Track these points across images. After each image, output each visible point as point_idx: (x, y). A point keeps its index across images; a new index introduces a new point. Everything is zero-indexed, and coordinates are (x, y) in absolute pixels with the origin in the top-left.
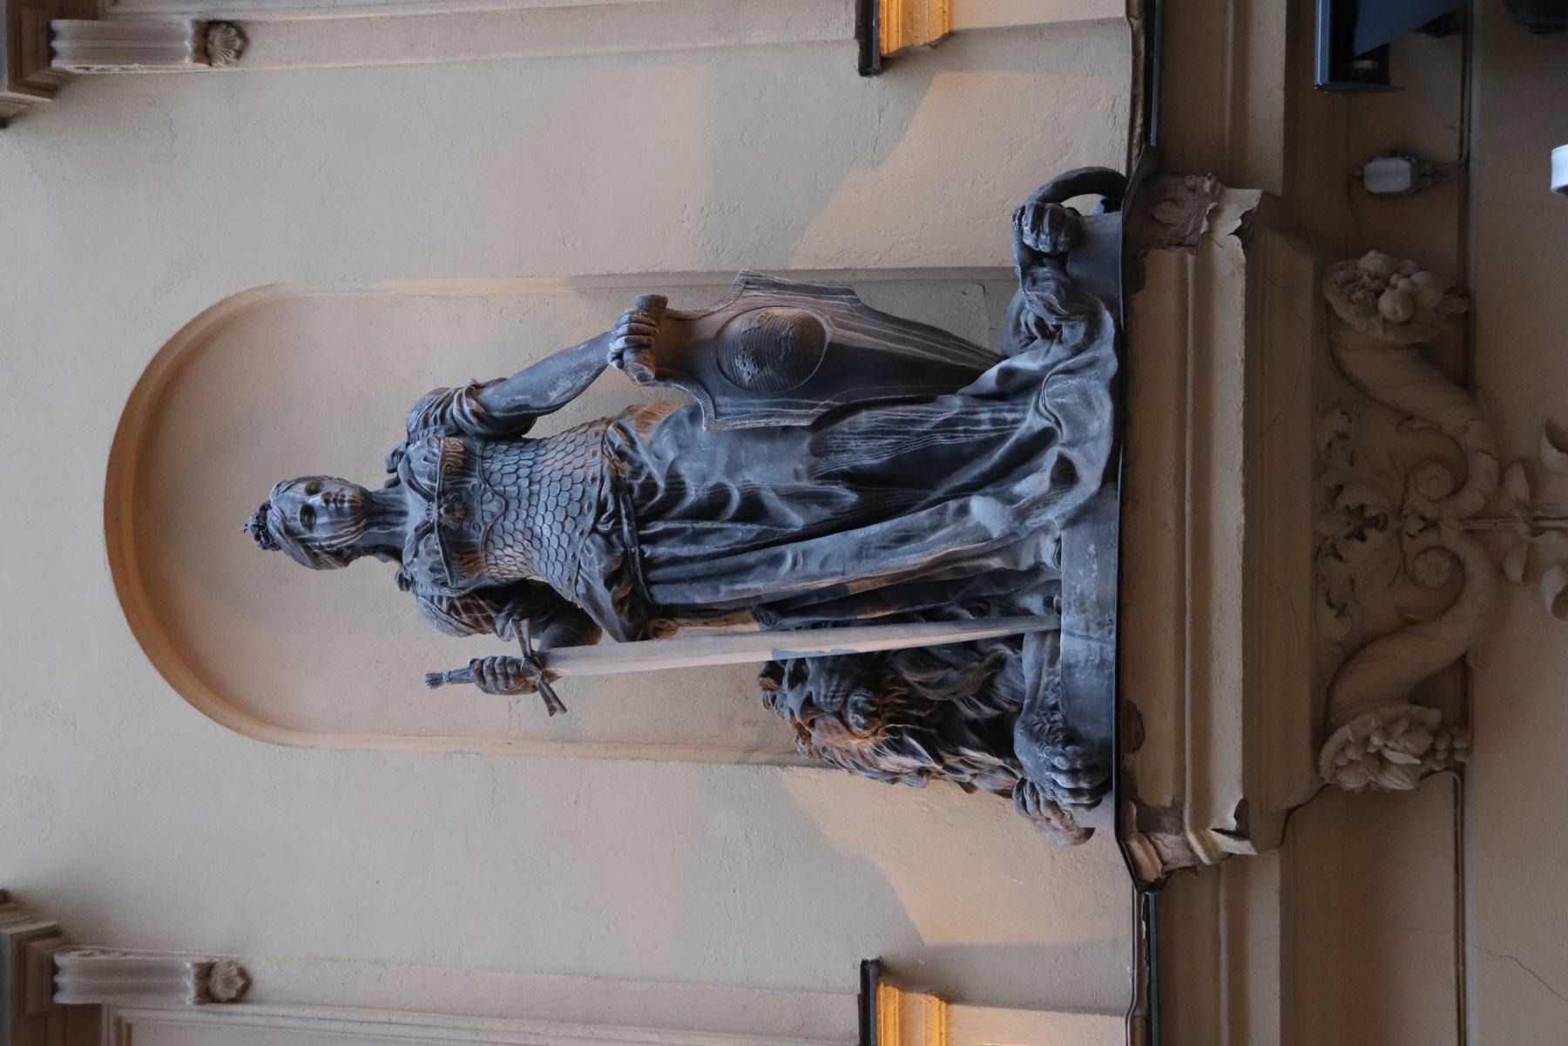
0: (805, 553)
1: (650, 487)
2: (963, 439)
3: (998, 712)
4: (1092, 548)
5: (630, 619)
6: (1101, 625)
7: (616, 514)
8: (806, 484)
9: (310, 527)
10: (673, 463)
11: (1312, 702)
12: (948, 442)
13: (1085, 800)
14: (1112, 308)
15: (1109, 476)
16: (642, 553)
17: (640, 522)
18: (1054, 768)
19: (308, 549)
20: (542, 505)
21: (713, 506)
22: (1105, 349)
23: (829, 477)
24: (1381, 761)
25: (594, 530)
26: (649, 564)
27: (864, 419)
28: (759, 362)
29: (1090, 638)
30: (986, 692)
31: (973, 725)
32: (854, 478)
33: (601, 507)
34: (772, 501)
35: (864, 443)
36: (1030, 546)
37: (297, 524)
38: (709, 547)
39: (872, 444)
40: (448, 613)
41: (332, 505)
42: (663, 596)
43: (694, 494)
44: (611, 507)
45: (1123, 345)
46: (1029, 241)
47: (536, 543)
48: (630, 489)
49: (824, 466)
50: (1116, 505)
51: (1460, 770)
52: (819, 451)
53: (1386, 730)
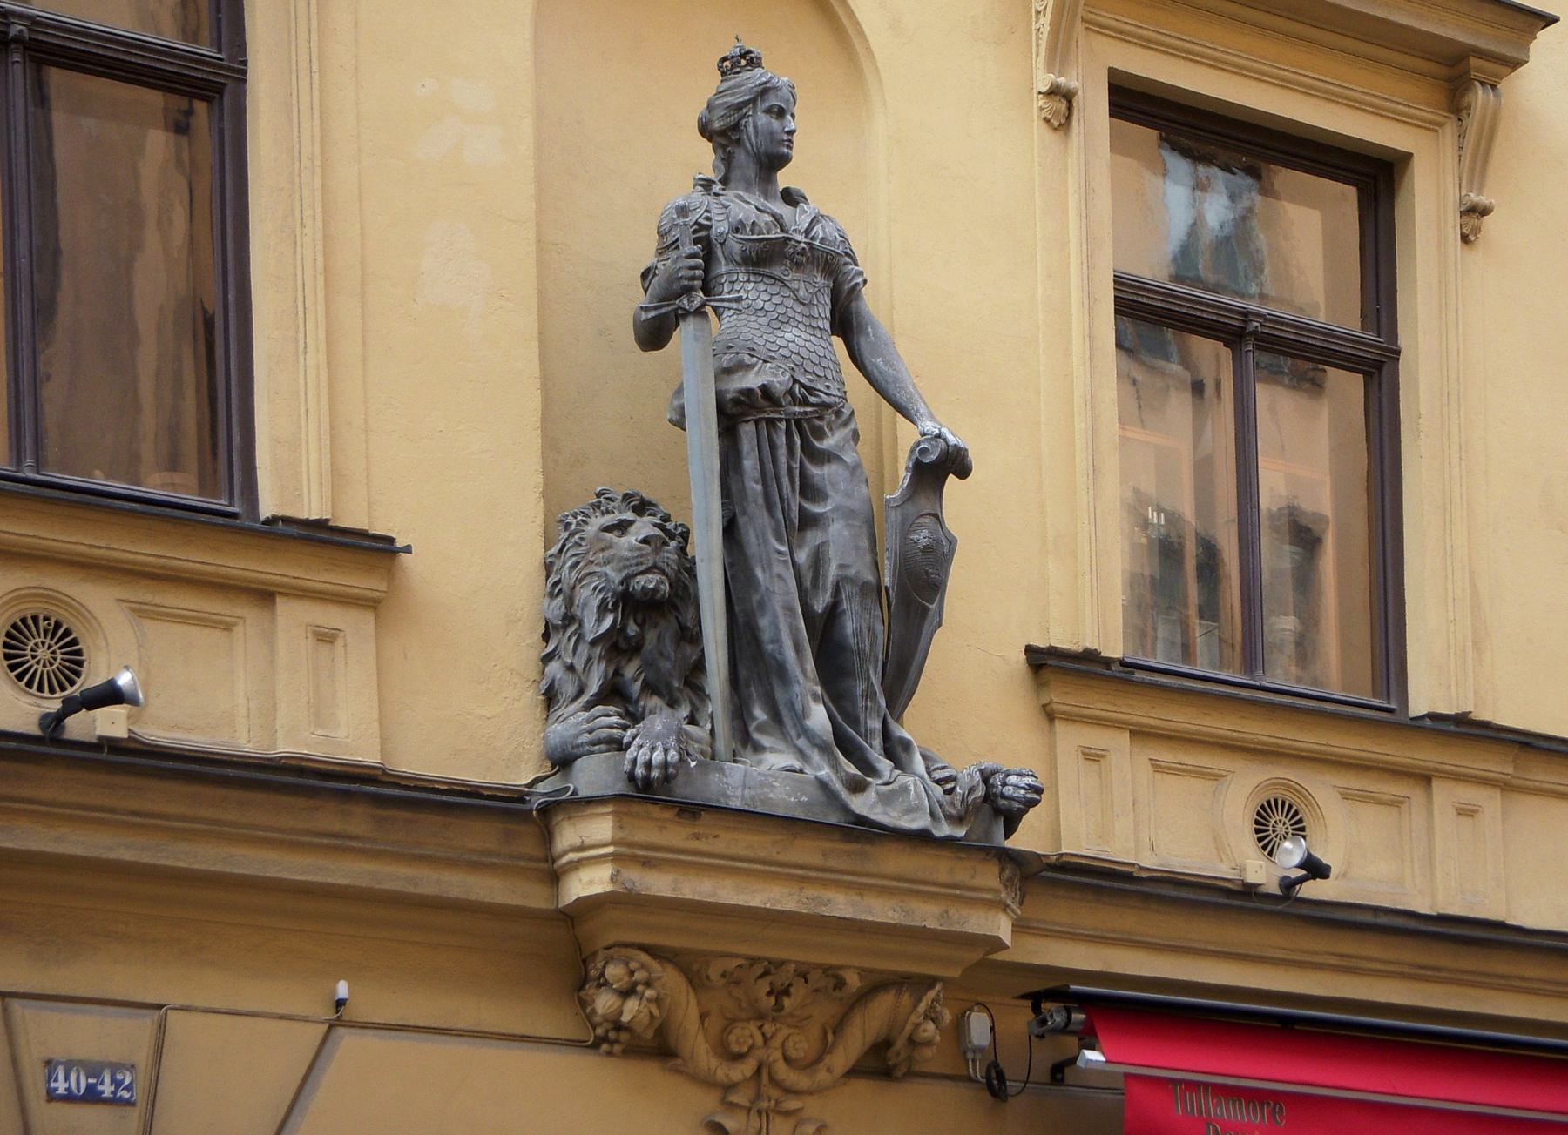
0: (785, 562)
1: (820, 435)
2: (860, 703)
3: (635, 696)
4: (804, 799)
5: (732, 399)
6: (752, 798)
7: (805, 402)
8: (832, 571)
9: (768, 111)
10: (840, 459)
11: (681, 945)
12: (859, 692)
13: (639, 771)
14: (965, 838)
15: (861, 820)
16: (780, 420)
17: (798, 423)
18: (653, 749)
19: (746, 103)
20: (808, 337)
21: (809, 490)
22: (944, 830)
23: (837, 591)
24: (627, 993)
25: (795, 381)
26: (772, 423)
27: (880, 628)
28: (927, 550)
29: (744, 787)
30: (650, 688)
31: (617, 673)
32: (833, 611)
33: (811, 390)
34: (814, 537)
35: (861, 626)
36: (781, 745)
37: (772, 101)
38: (786, 481)
39: (865, 632)
40: (696, 223)
41: (785, 137)
42: (747, 431)
43: (816, 472)
44: (812, 399)
45: (949, 842)
46: (1013, 779)
47: (775, 324)
48: (821, 418)
49: (847, 590)
50: (833, 820)
51: (595, 1046)
52: (864, 588)
53: (657, 1001)
